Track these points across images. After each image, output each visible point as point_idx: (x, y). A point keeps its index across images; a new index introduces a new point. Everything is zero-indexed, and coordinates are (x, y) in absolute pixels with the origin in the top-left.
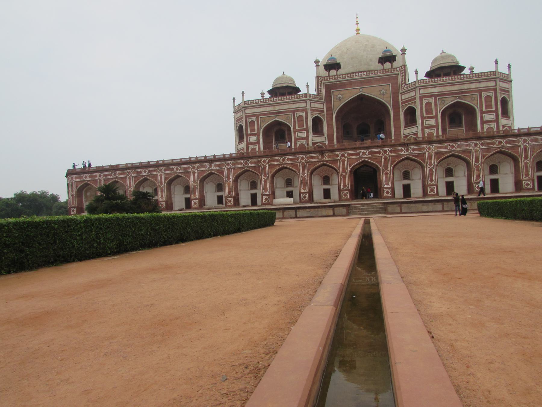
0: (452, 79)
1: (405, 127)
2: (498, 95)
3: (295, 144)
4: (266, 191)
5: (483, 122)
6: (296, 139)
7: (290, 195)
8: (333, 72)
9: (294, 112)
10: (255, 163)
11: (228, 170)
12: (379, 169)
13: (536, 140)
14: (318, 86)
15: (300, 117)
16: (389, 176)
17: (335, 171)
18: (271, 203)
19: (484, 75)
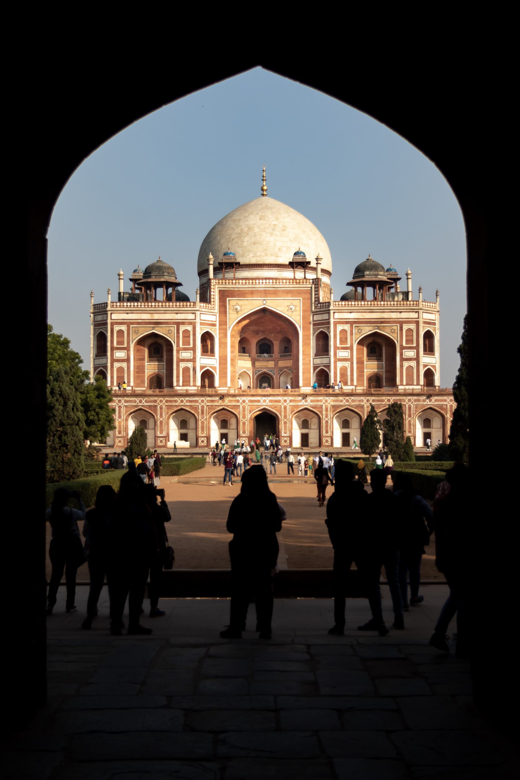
0: (371, 304)
1: (316, 355)
2: (421, 329)
3: (178, 366)
4: (161, 433)
5: (402, 360)
7: (184, 437)
9: (178, 324)
10: (151, 402)
11: (120, 407)
13: (419, 400)
15: (186, 332)
16: (287, 425)
17: (234, 416)
18: (165, 446)
19: (407, 304)
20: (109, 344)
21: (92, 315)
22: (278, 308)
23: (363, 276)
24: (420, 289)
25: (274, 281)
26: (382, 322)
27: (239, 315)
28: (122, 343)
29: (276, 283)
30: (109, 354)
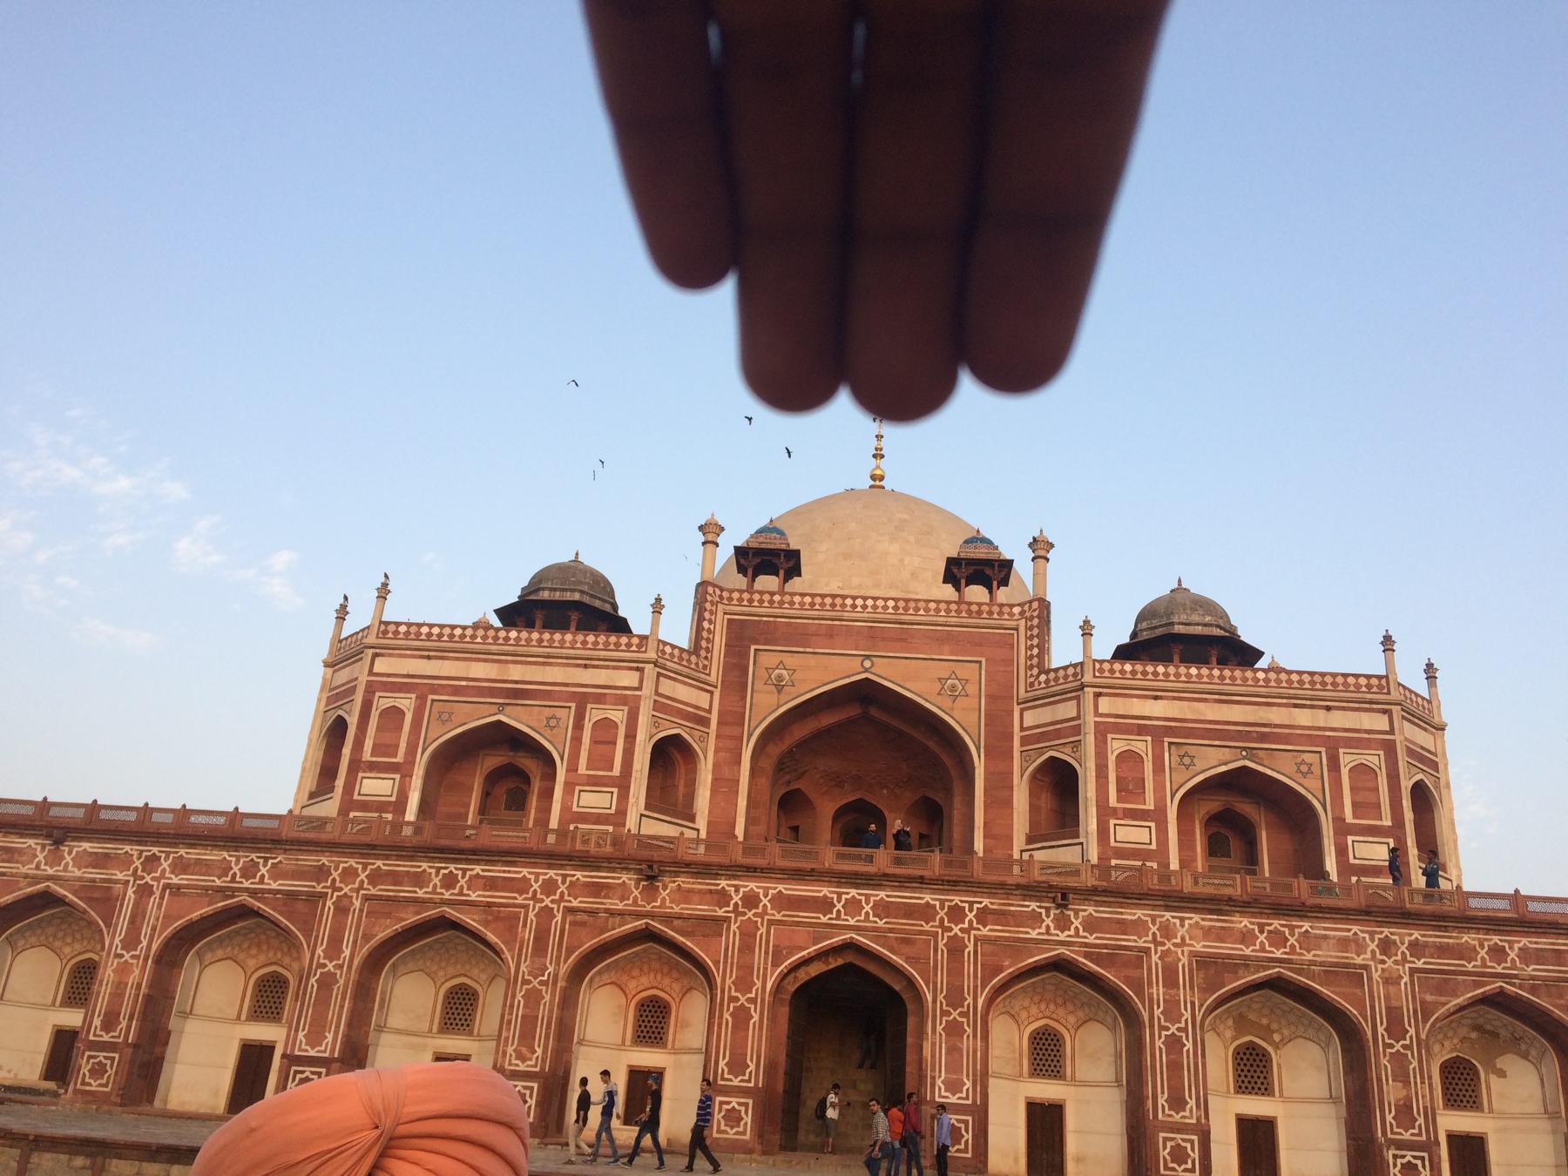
0: (1222, 677)
1: (1030, 839)
4: (315, 1038)
5: (1345, 868)
6: (569, 815)
8: (768, 582)
9: (582, 700)
11: (145, 891)
12: (918, 997)
14: (700, 619)
15: (606, 725)
16: (966, 1044)
19: (1346, 684)
20: (346, 751)
21: (330, 670)
22: (907, 685)
23: (1172, 624)
24: (1388, 643)
25: (901, 604)
26: (1263, 737)
27: (784, 698)
28: (392, 749)
29: (906, 609)
30: (340, 782)
